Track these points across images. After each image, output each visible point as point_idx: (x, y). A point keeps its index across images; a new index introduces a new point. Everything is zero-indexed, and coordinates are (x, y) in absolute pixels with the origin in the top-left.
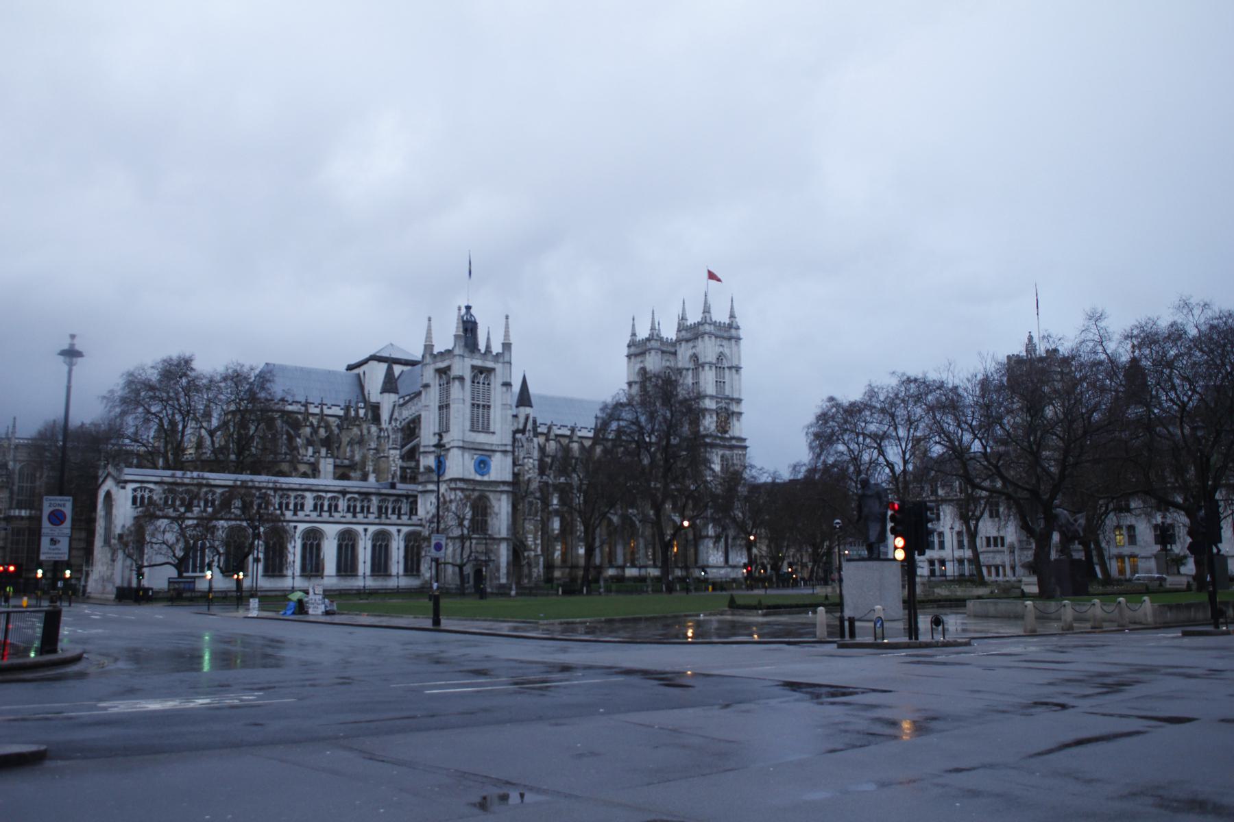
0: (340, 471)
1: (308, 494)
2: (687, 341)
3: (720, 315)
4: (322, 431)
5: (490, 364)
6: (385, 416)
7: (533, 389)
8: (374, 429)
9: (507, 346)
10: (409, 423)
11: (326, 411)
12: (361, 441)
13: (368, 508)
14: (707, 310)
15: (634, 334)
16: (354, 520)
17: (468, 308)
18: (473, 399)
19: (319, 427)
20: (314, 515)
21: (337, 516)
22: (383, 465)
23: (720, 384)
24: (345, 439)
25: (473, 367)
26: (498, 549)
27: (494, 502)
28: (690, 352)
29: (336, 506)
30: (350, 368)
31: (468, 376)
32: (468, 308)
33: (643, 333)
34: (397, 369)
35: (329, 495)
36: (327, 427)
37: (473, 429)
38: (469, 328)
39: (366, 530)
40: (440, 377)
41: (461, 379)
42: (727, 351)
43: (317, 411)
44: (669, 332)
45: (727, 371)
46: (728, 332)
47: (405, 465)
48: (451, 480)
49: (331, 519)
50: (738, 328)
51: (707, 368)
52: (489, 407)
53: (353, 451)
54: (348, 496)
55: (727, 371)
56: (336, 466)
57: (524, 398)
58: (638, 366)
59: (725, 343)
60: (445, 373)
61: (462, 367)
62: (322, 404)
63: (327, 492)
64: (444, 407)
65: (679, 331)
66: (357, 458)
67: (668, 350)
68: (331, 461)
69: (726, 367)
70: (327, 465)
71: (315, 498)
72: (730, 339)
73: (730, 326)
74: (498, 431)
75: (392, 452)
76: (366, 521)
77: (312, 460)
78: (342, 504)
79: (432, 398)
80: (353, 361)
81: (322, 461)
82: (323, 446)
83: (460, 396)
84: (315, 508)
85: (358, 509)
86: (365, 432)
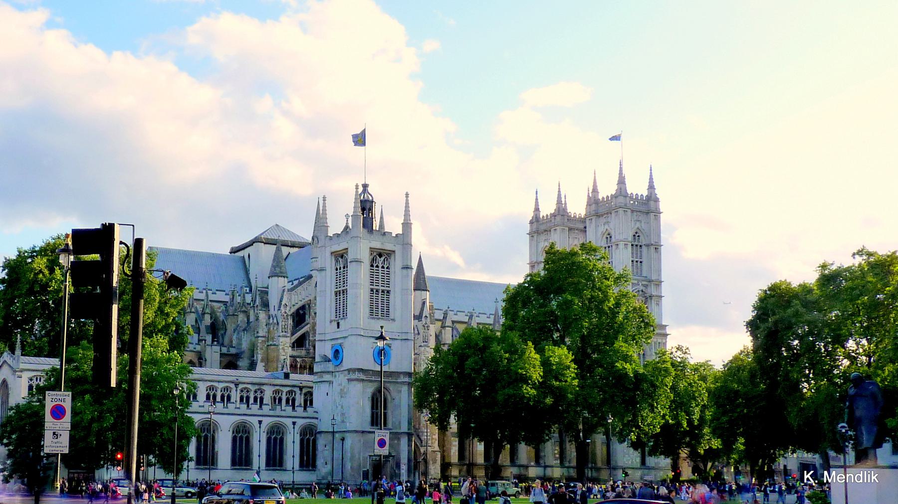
0: (226, 360)
1: (199, 384)
2: (598, 215)
3: (637, 187)
5: (389, 247)
6: (273, 301)
7: (428, 273)
8: (262, 315)
9: (407, 225)
10: (298, 310)
12: (248, 327)
13: (262, 399)
14: (622, 181)
16: (249, 412)
17: (365, 186)
18: (372, 283)
19: (203, 314)
20: (208, 407)
21: (231, 408)
22: (272, 354)
23: (637, 263)
24: (230, 327)
25: (372, 250)
26: (399, 444)
27: (394, 394)
28: (602, 229)
29: (229, 398)
30: (234, 251)
31: (366, 258)
32: (365, 186)
34: (285, 250)
36: (213, 314)
37: (373, 313)
38: (366, 206)
39: (260, 422)
40: (337, 261)
41: (358, 261)
43: (202, 296)
45: (644, 249)
46: (647, 208)
47: (295, 353)
48: (349, 370)
49: (225, 411)
50: (657, 200)
51: (621, 245)
52: (388, 292)
53: (240, 339)
54: (241, 386)
56: (222, 355)
57: (421, 283)
59: (642, 217)
60: (342, 257)
61: (361, 249)
64: (341, 293)
65: (589, 204)
66: (245, 346)
67: (578, 226)
68: (217, 348)
69: (646, 244)
70: (213, 353)
73: (649, 198)
75: (281, 339)
76: (260, 412)
77: (198, 348)
78: (235, 396)
79: (326, 282)
80: (237, 244)
81: (208, 349)
83: (360, 278)
85: (251, 401)
86: (252, 319)
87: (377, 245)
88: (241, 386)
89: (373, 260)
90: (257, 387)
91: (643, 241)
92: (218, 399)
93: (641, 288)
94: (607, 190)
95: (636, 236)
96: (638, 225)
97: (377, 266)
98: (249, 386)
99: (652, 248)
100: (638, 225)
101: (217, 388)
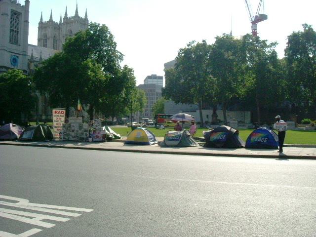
15: (41, 19)
33: (46, 19)
37: (11, 42)
44: (57, 20)
52: (18, 32)
58: (43, 33)
74: (21, 45)
87: (15, 9)
89: (12, 15)
94: (71, 14)
97: (14, 19)
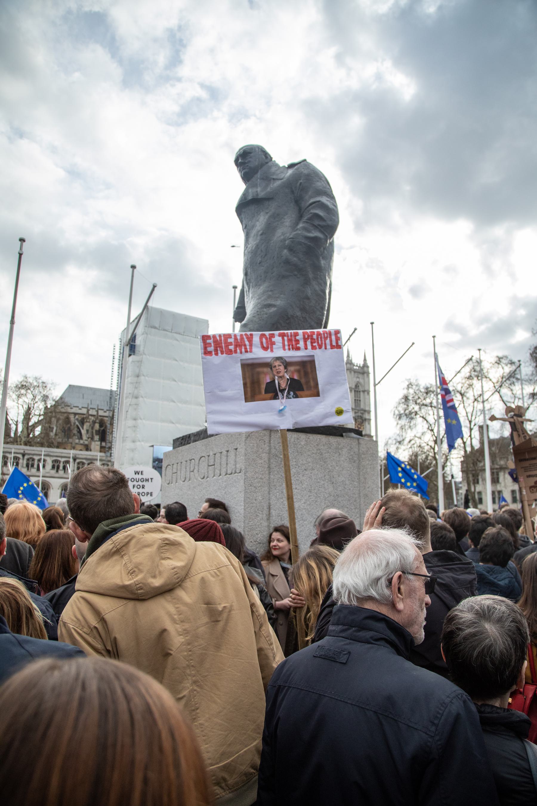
4: (97, 426)
11: (101, 413)
35: (63, 460)
42: (361, 381)
43: (94, 413)
49: (57, 475)
55: (362, 393)
59: (360, 376)
62: (98, 409)
63: (62, 457)
71: (53, 461)
72: (363, 373)
77: (86, 443)
81: (93, 443)
82: (96, 434)
84: (53, 467)
88: (78, 461)
90: (89, 462)
91: (361, 389)
92: (61, 468)
93: (360, 414)
95: (357, 386)
96: (358, 380)
98: (84, 461)
99: (366, 393)
100: (358, 380)
101: (60, 462)
